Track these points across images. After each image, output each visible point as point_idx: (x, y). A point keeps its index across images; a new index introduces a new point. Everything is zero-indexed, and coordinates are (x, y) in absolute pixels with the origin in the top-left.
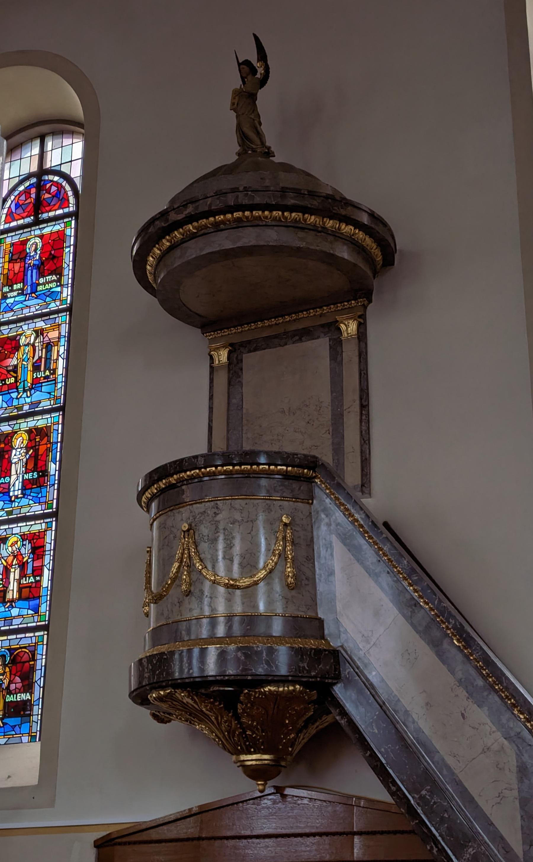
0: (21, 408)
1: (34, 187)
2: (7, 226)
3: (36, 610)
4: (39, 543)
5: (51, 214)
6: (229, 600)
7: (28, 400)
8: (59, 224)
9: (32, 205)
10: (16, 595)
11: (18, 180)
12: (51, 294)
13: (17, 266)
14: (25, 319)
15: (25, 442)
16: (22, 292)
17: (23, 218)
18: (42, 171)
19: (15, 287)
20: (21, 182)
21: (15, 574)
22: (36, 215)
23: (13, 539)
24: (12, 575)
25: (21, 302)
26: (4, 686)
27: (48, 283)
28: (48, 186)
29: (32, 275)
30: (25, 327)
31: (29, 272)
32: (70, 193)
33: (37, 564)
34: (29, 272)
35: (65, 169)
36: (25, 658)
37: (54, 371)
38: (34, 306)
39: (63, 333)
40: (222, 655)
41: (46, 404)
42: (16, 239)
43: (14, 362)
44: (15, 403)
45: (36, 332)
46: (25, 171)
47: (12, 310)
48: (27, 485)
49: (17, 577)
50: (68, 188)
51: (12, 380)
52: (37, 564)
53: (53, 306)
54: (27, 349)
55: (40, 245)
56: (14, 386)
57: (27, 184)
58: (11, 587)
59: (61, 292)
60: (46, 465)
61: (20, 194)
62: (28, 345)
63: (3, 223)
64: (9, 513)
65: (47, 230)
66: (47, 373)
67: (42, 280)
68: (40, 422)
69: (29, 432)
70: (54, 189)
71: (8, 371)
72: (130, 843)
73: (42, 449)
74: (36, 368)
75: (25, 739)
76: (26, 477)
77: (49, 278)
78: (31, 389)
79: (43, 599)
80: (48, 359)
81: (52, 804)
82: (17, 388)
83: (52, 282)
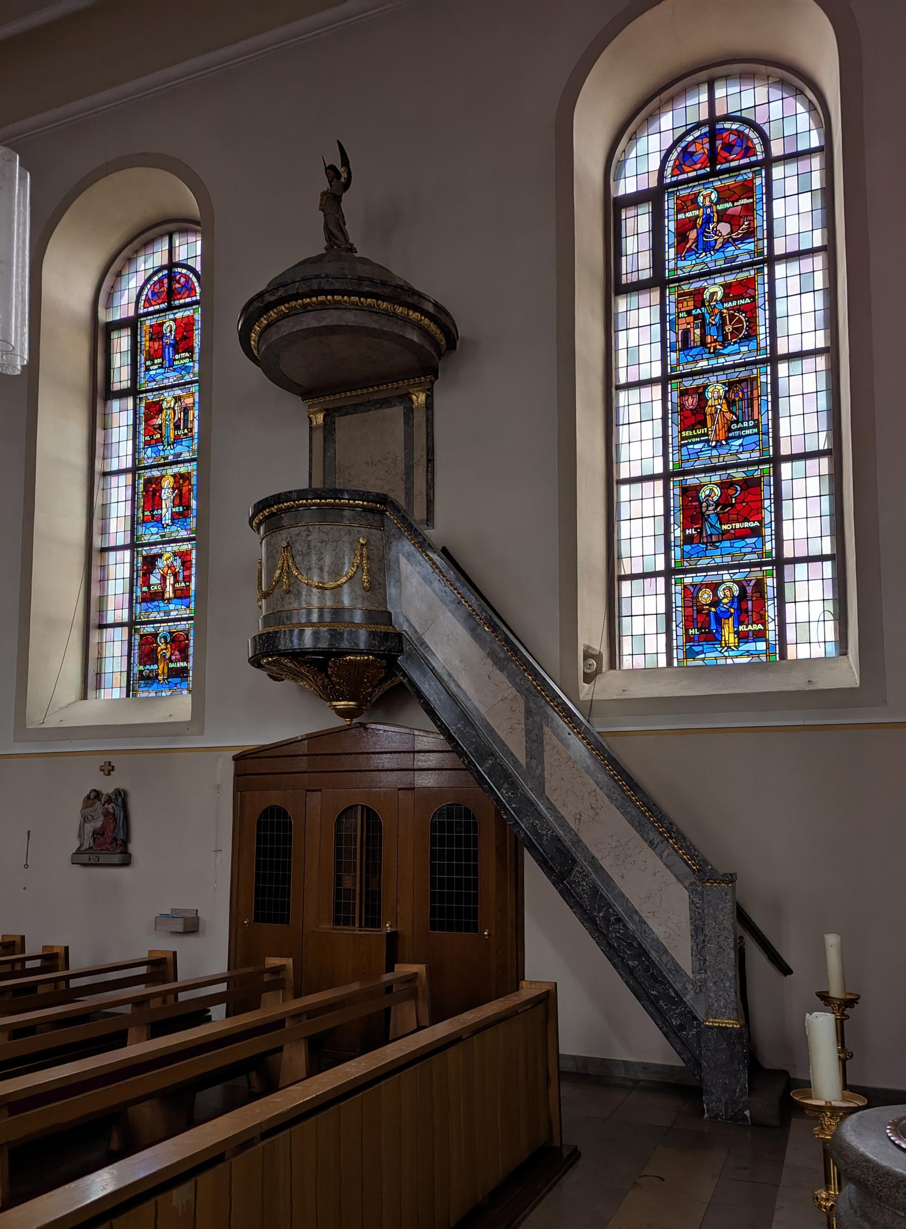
0: (166, 458)
3: (188, 607)
4: (187, 558)
5: (182, 301)
6: (322, 597)
7: (172, 452)
10: (172, 595)
12: (185, 368)
13: (156, 345)
14: (165, 388)
15: (172, 484)
16: (161, 366)
17: (159, 304)
18: (172, 265)
19: (156, 361)
21: (170, 580)
23: (166, 556)
25: (162, 374)
26: (167, 657)
27: (183, 359)
30: (166, 394)
33: (186, 573)
35: (191, 263)
36: (182, 638)
37: (191, 430)
38: (172, 377)
40: (316, 636)
41: (186, 455)
42: (154, 322)
43: (159, 422)
44: (162, 454)
46: (158, 264)
47: (155, 380)
48: (175, 517)
49: (172, 582)
51: (158, 436)
52: (186, 573)
53: (188, 378)
54: (169, 411)
55: (174, 327)
56: (160, 441)
57: (160, 275)
59: (194, 367)
61: (155, 284)
62: (169, 408)
64: (162, 536)
66: (186, 431)
67: (177, 357)
68: (182, 469)
69: (174, 476)
70: (183, 280)
71: (155, 429)
72: (257, 758)
73: (185, 489)
74: (177, 427)
76: (174, 510)
77: (183, 355)
78: (173, 443)
80: (186, 420)
81: (201, 732)
82: (162, 442)
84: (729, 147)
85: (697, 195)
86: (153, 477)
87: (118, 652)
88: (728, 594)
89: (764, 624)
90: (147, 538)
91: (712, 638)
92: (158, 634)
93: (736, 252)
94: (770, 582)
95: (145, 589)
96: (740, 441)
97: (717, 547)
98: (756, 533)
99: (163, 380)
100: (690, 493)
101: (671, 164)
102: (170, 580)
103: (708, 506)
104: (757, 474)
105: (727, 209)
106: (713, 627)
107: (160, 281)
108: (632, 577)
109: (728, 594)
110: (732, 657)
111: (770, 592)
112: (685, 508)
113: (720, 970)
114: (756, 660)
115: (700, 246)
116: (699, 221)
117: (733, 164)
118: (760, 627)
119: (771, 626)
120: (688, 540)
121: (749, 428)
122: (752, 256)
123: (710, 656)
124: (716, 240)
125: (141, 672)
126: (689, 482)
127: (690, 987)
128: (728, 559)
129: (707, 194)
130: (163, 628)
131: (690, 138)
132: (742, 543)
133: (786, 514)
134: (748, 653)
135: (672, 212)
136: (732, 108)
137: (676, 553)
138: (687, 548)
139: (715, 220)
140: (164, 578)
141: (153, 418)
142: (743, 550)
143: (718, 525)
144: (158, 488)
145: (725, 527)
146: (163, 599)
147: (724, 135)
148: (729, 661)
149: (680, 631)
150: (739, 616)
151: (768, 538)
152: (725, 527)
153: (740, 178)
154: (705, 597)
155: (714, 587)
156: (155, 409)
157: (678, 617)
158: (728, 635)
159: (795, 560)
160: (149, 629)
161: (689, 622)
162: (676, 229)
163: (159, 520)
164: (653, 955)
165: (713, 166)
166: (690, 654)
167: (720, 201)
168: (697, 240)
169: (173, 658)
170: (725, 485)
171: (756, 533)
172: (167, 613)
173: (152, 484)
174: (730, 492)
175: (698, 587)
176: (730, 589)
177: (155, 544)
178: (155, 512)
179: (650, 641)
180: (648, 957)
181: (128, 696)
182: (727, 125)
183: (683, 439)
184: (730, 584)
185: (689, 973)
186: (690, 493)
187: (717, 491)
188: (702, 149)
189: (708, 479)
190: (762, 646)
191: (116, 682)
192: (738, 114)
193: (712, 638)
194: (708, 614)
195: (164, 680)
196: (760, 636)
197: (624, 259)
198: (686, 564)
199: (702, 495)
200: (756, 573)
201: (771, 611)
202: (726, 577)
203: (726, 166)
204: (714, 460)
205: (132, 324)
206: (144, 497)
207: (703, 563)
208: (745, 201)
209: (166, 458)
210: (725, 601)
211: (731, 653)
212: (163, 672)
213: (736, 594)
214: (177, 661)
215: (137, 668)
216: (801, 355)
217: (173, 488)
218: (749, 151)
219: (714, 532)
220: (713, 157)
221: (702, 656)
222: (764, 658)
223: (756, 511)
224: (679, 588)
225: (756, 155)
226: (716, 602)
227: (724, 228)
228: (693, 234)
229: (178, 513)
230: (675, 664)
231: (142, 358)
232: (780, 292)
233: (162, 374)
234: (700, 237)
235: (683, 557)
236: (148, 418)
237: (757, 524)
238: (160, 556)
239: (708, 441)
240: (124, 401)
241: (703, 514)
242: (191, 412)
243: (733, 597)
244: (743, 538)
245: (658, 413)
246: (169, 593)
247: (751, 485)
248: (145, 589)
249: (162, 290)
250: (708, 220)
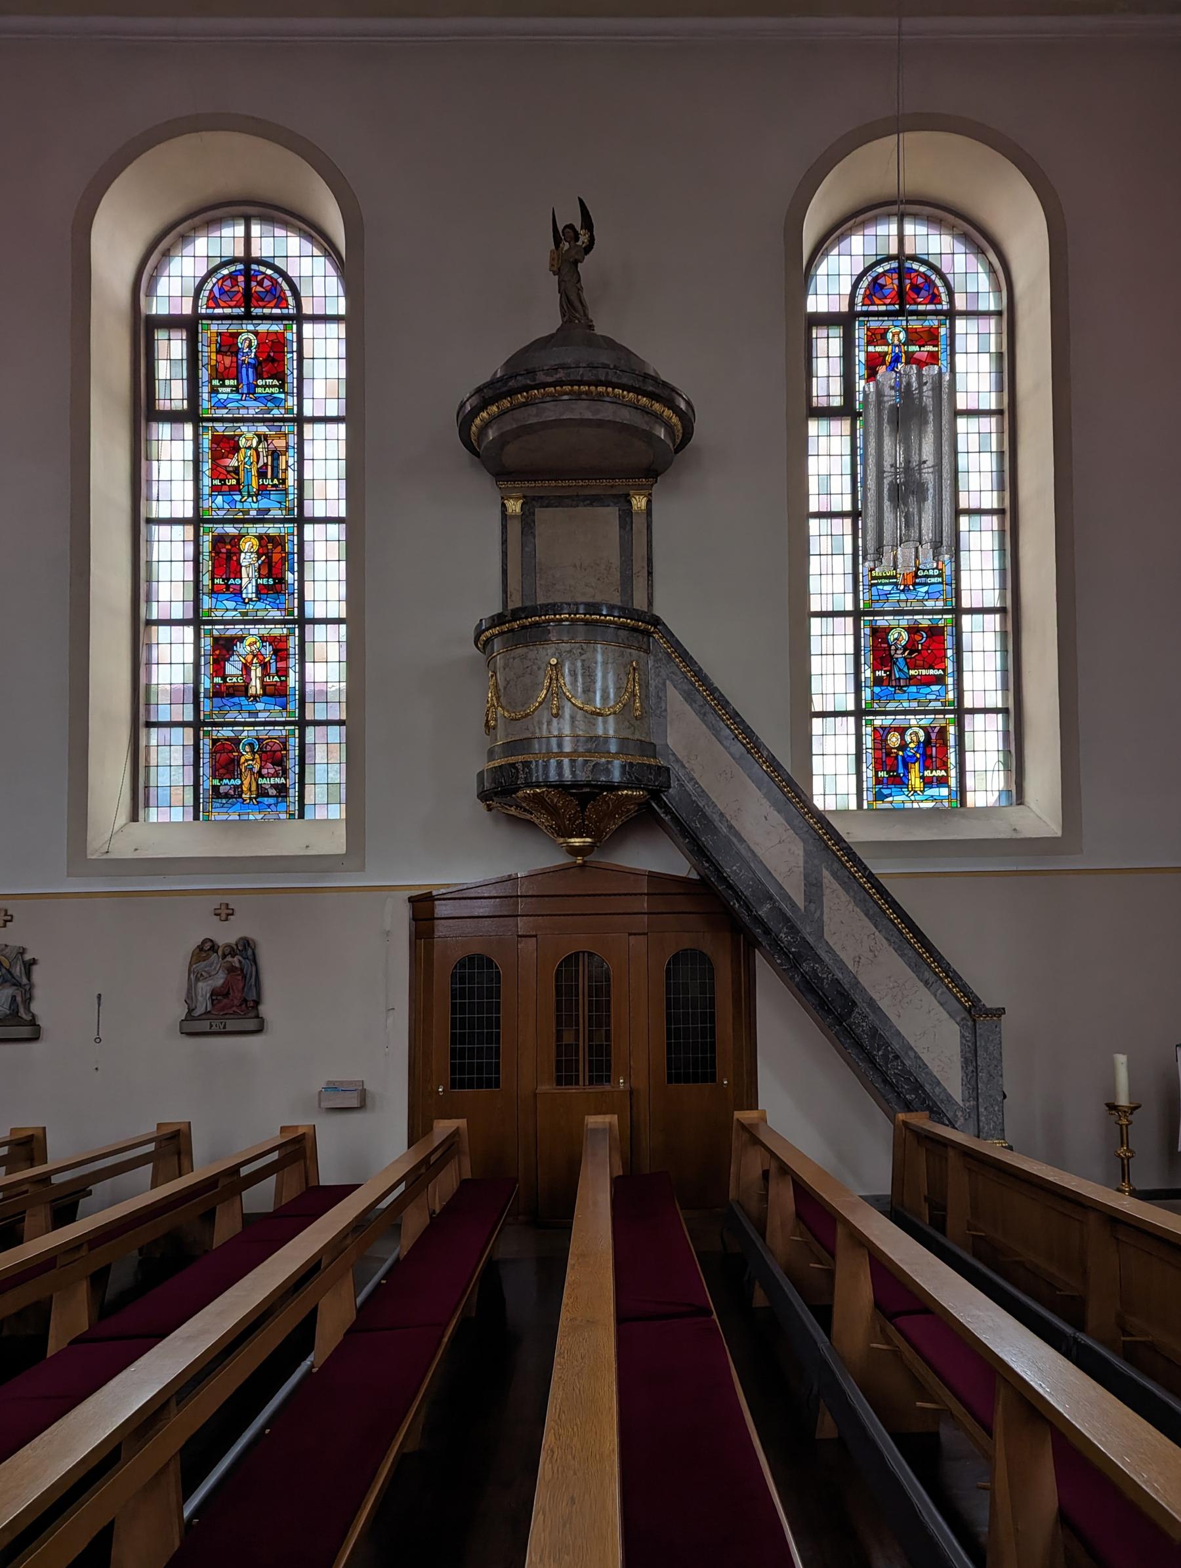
0: (247, 512)
2: (210, 311)
3: (285, 708)
4: (281, 646)
5: (267, 311)
7: (255, 506)
9: (240, 295)
10: (260, 691)
12: (273, 399)
13: (228, 361)
14: (243, 420)
15: (256, 548)
16: (236, 389)
17: (230, 307)
19: (227, 382)
21: (256, 672)
22: (248, 308)
23: (250, 640)
24: (253, 673)
25: (237, 401)
26: (256, 770)
27: (269, 386)
28: (259, 278)
29: (248, 375)
30: (244, 429)
31: (244, 370)
32: (288, 293)
33: (281, 665)
34: (244, 370)
35: (278, 262)
36: (276, 748)
37: (284, 481)
38: (253, 409)
39: (291, 444)
41: (276, 513)
42: (223, 328)
44: (239, 506)
45: (259, 436)
46: (228, 252)
49: (259, 674)
50: (285, 286)
51: (234, 482)
52: (281, 665)
53: (276, 413)
54: (249, 452)
55: (255, 343)
56: (236, 488)
57: (233, 269)
58: (253, 683)
59: (286, 400)
60: (283, 573)
61: (224, 278)
62: (250, 448)
64: (246, 614)
65: (263, 327)
66: (275, 481)
67: (260, 382)
68: (272, 530)
69: (260, 538)
70: (267, 283)
71: (229, 472)
73: (276, 557)
74: (262, 474)
75: (283, 816)
76: (260, 581)
77: (269, 381)
78: (257, 495)
79: (291, 698)
80: (275, 468)
81: (362, 868)
82: (240, 491)
83: (275, 386)
84: (916, 289)
85: (886, 331)
86: (227, 535)
87: (177, 759)
88: (915, 738)
89: (946, 771)
90: (219, 613)
91: (899, 782)
92: (240, 741)
94: (952, 730)
95: (218, 680)
96: (925, 589)
97: (905, 692)
98: (940, 680)
99: (238, 408)
100: (879, 634)
101: (862, 291)
102: (256, 672)
103: (896, 649)
104: (941, 624)
105: (914, 353)
106: (901, 770)
107: (232, 277)
108: (823, 715)
109: (915, 738)
110: (918, 802)
111: (952, 741)
112: (875, 649)
113: (991, 1096)
114: (939, 805)
116: (888, 358)
117: (921, 308)
118: (943, 773)
119: (953, 773)
120: (878, 682)
121: (934, 576)
123: (899, 799)
125: (215, 789)
126: (879, 623)
127: (959, 1114)
128: (914, 705)
129: (896, 331)
130: (247, 733)
131: (880, 270)
132: (927, 690)
133: (966, 666)
134: (932, 798)
135: (863, 342)
136: (920, 250)
137: (866, 694)
138: (877, 690)
140: (246, 668)
141: (223, 457)
142: (929, 697)
143: (906, 670)
144: (234, 550)
145: (912, 672)
146: (246, 695)
147: (913, 275)
148: (915, 805)
149: (870, 773)
150: (924, 762)
151: (950, 687)
152: (912, 672)
153: (927, 323)
154: (894, 740)
155: (902, 731)
156: (226, 446)
157: (868, 758)
158: (915, 781)
159: (974, 711)
160: (226, 732)
161: (879, 765)
162: (867, 361)
163: (238, 592)
164: (927, 1087)
165: (902, 305)
166: (879, 797)
167: (908, 342)
169: (264, 771)
170: (913, 630)
171: (940, 680)
172: (255, 713)
173: (225, 543)
174: (917, 637)
175: (887, 730)
176: (916, 734)
177: (233, 622)
178: (231, 581)
179: (841, 780)
180: (924, 1091)
181: (196, 818)
182: (915, 266)
183: (873, 578)
184: (917, 729)
185: (961, 1103)
186: (879, 634)
187: (905, 635)
188: (891, 283)
189: (896, 623)
190: (944, 791)
191: (177, 799)
192: (925, 257)
193: (899, 782)
194: (896, 758)
195: (251, 799)
196: (943, 782)
197: (814, 380)
198: (875, 705)
199: (891, 638)
200: (940, 721)
201: (952, 758)
202: (913, 722)
203: (913, 307)
204: (903, 604)
205: (189, 325)
206: (212, 558)
207: (891, 706)
208: (930, 348)
209: (247, 512)
210: (912, 745)
211: (918, 798)
212: (250, 790)
213: (922, 739)
214: (269, 776)
215: (207, 783)
216: (980, 512)
217: (257, 552)
218: (934, 298)
219: (902, 676)
220: (901, 296)
221: (890, 799)
222: (946, 804)
223: (937, 660)
224: (869, 730)
225: (940, 303)
226: (903, 746)
229: (267, 587)
230: (865, 807)
231: (204, 374)
232: (961, 447)
233: (237, 401)
235: (872, 699)
236: (216, 457)
237: (941, 672)
238: (241, 639)
239: (896, 584)
240: (178, 426)
241: (892, 657)
242: (283, 459)
243: (919, 742)
244: (928, 685)
245: (849, 549)
246: (255, 686)
247: (935, 633)
248: (218, 680)
249: (235, 289)
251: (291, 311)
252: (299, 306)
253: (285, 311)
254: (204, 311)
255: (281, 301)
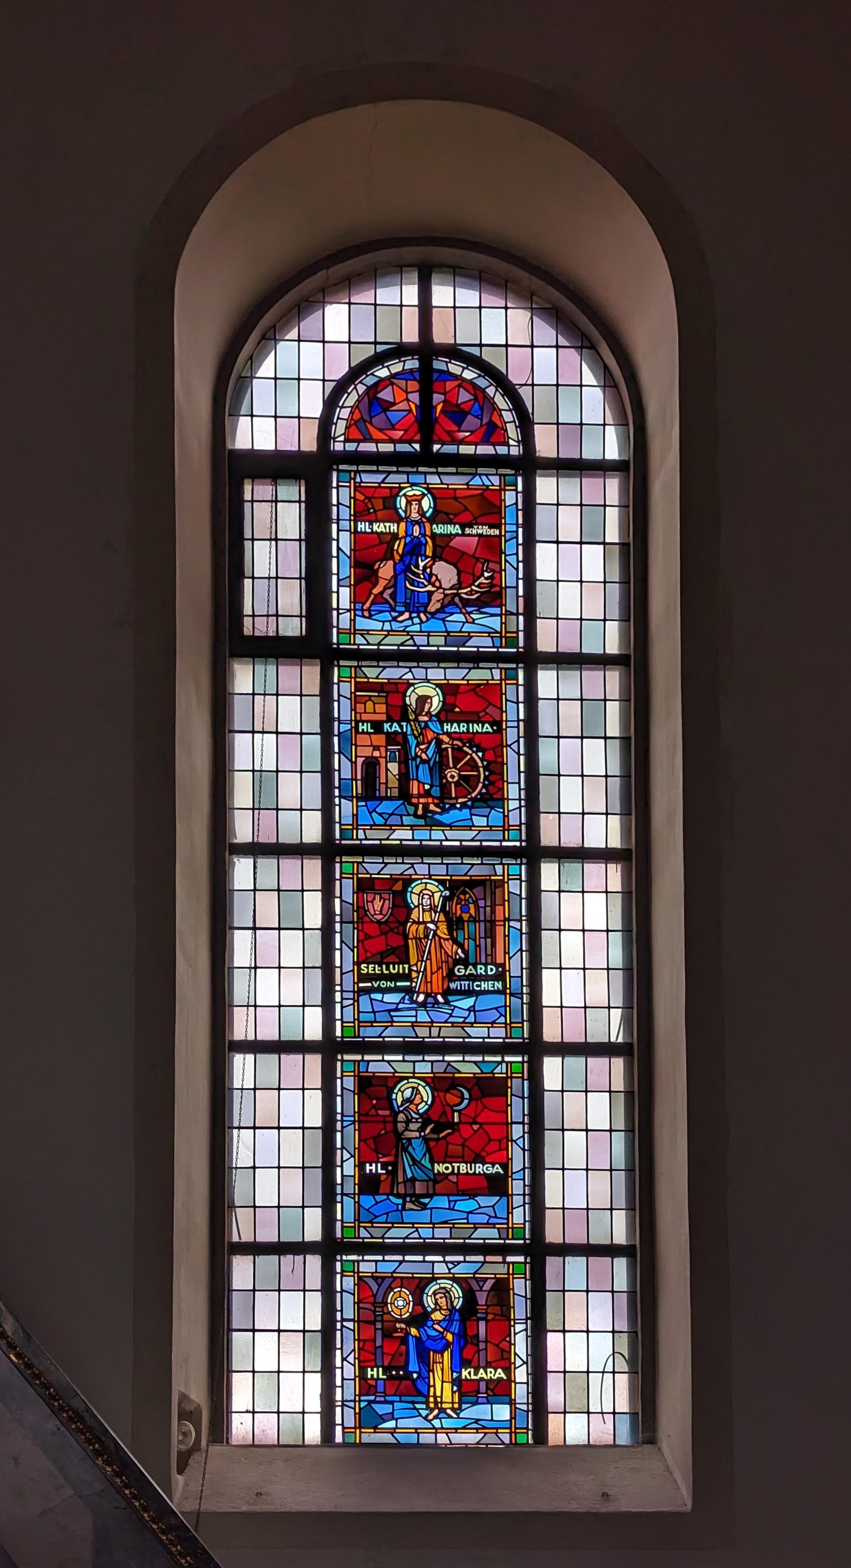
1: (415, 379)
2: (351, 447)
8: (487, 475)
11: (373, 353)
20: (379, 359)
22: (426, 444)
46: (389, 335)
50: (501, 402)
57: (397, 367)
63: (342, 438)
93: (468, 628)
115: (400, 598)
122: (498, 644)
124: (430, 594)
139: (429, 552)
168: (394, 583)
227: (447, 574)
228: (386, 570)
234: (401, 578)
250: (415, 549)
251: (515, 451)
252: (527, 439)
253: (502, 450)
254: (339, 447)
255: (492, 432)
